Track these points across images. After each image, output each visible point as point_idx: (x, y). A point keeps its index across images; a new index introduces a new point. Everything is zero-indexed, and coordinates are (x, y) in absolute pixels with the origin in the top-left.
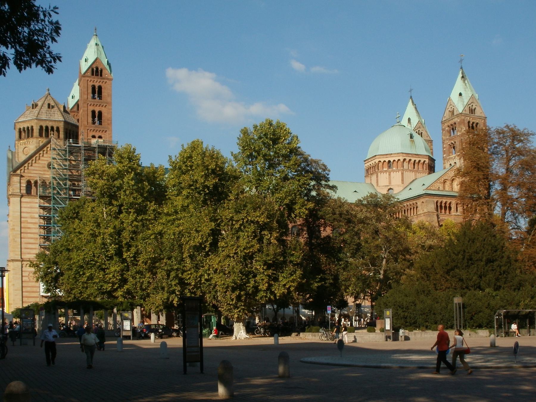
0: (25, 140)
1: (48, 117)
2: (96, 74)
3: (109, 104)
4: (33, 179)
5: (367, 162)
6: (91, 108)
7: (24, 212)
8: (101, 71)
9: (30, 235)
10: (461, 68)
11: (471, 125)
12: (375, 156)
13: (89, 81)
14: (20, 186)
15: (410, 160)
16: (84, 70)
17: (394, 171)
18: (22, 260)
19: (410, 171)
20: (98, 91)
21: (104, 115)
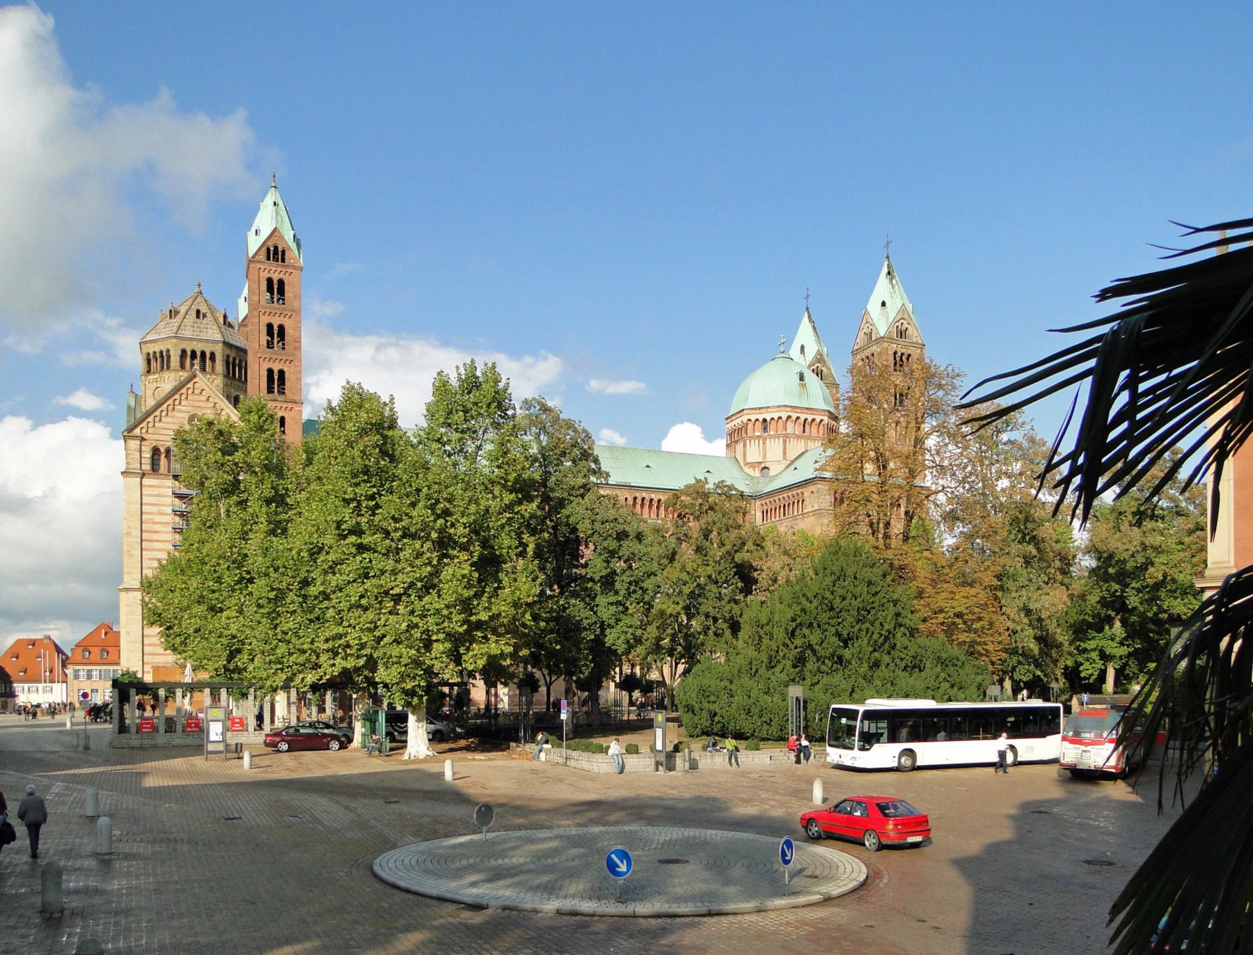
1: (195, 333)
3: (297, 311)
4: (163, 445)
5: (729, 420)
6: (266, 320)
7: (146, 504)
8: (283, 252)
9: (156, 545)
10: (888, 257)
11: (898, 359)
12: (743, 410)
13: (261, 270)
15: (798, 418)
16: (252, 250)
17: (771, 437)
19: (798, 437)
20: (278, 288)
21: (289, 332)
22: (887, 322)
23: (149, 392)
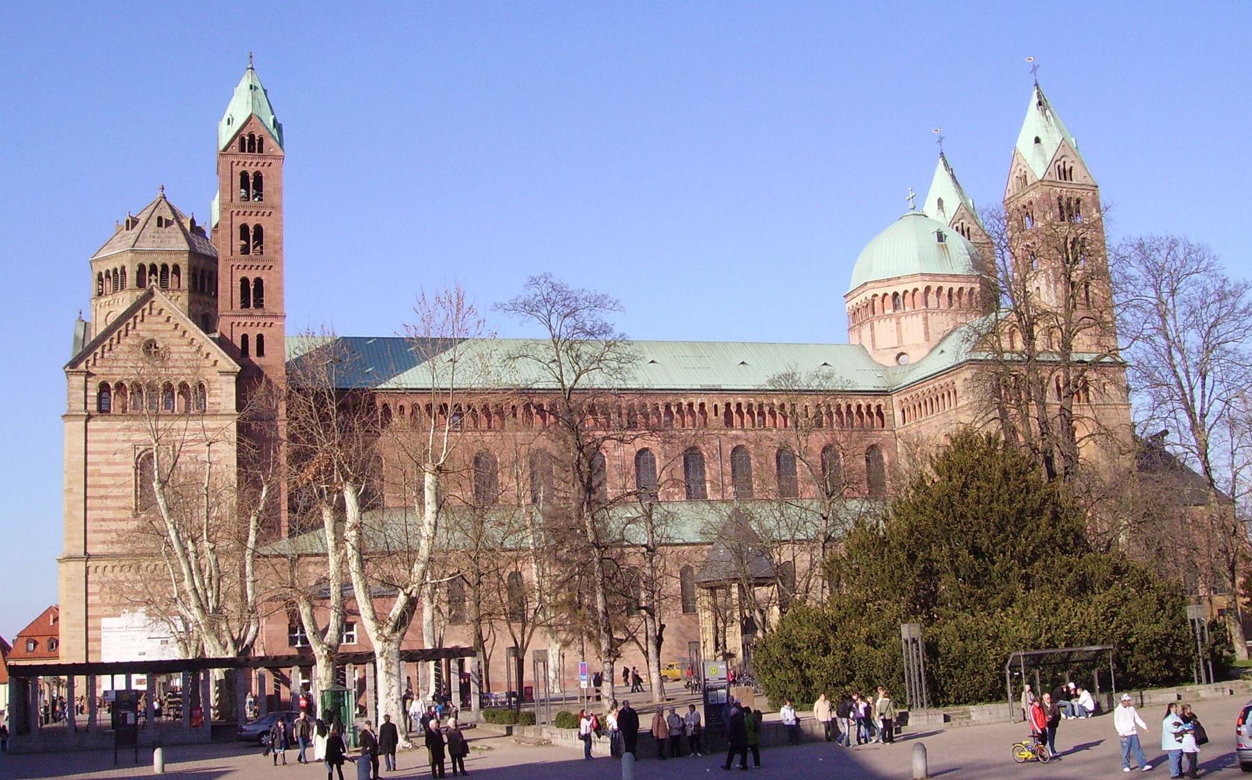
0: (110, 298)
1: (155, 245)
2: (249, 148)
3: (277, 208)
4: (112, 380)
6: (239, 221)
8: (261, 140)
10: (1037, 85)
12: (866, 284)
13: (234, 164)
14: (86, 396)
15: (940, 289)
16: (224, 140)
17: (906, 314)
18: (88, 557)
19: (943, 312)
22: (1045, 162)
23: (101, 319)
